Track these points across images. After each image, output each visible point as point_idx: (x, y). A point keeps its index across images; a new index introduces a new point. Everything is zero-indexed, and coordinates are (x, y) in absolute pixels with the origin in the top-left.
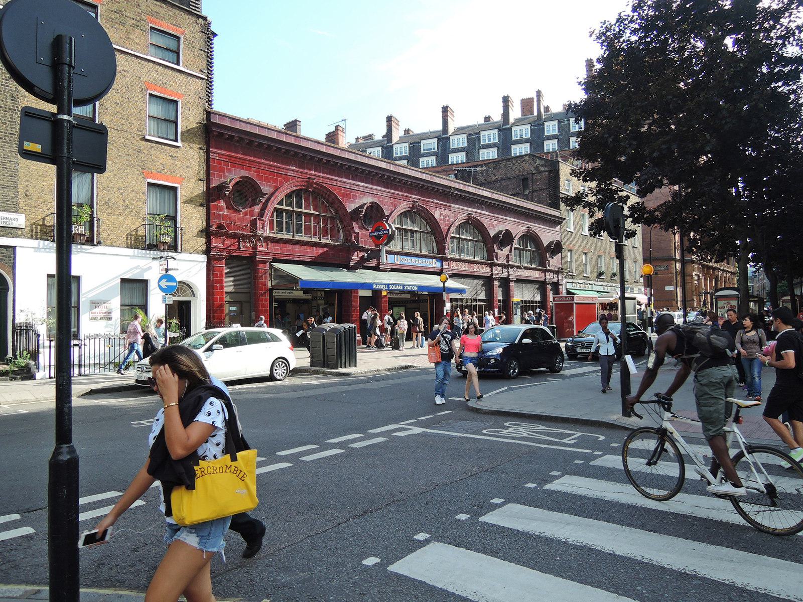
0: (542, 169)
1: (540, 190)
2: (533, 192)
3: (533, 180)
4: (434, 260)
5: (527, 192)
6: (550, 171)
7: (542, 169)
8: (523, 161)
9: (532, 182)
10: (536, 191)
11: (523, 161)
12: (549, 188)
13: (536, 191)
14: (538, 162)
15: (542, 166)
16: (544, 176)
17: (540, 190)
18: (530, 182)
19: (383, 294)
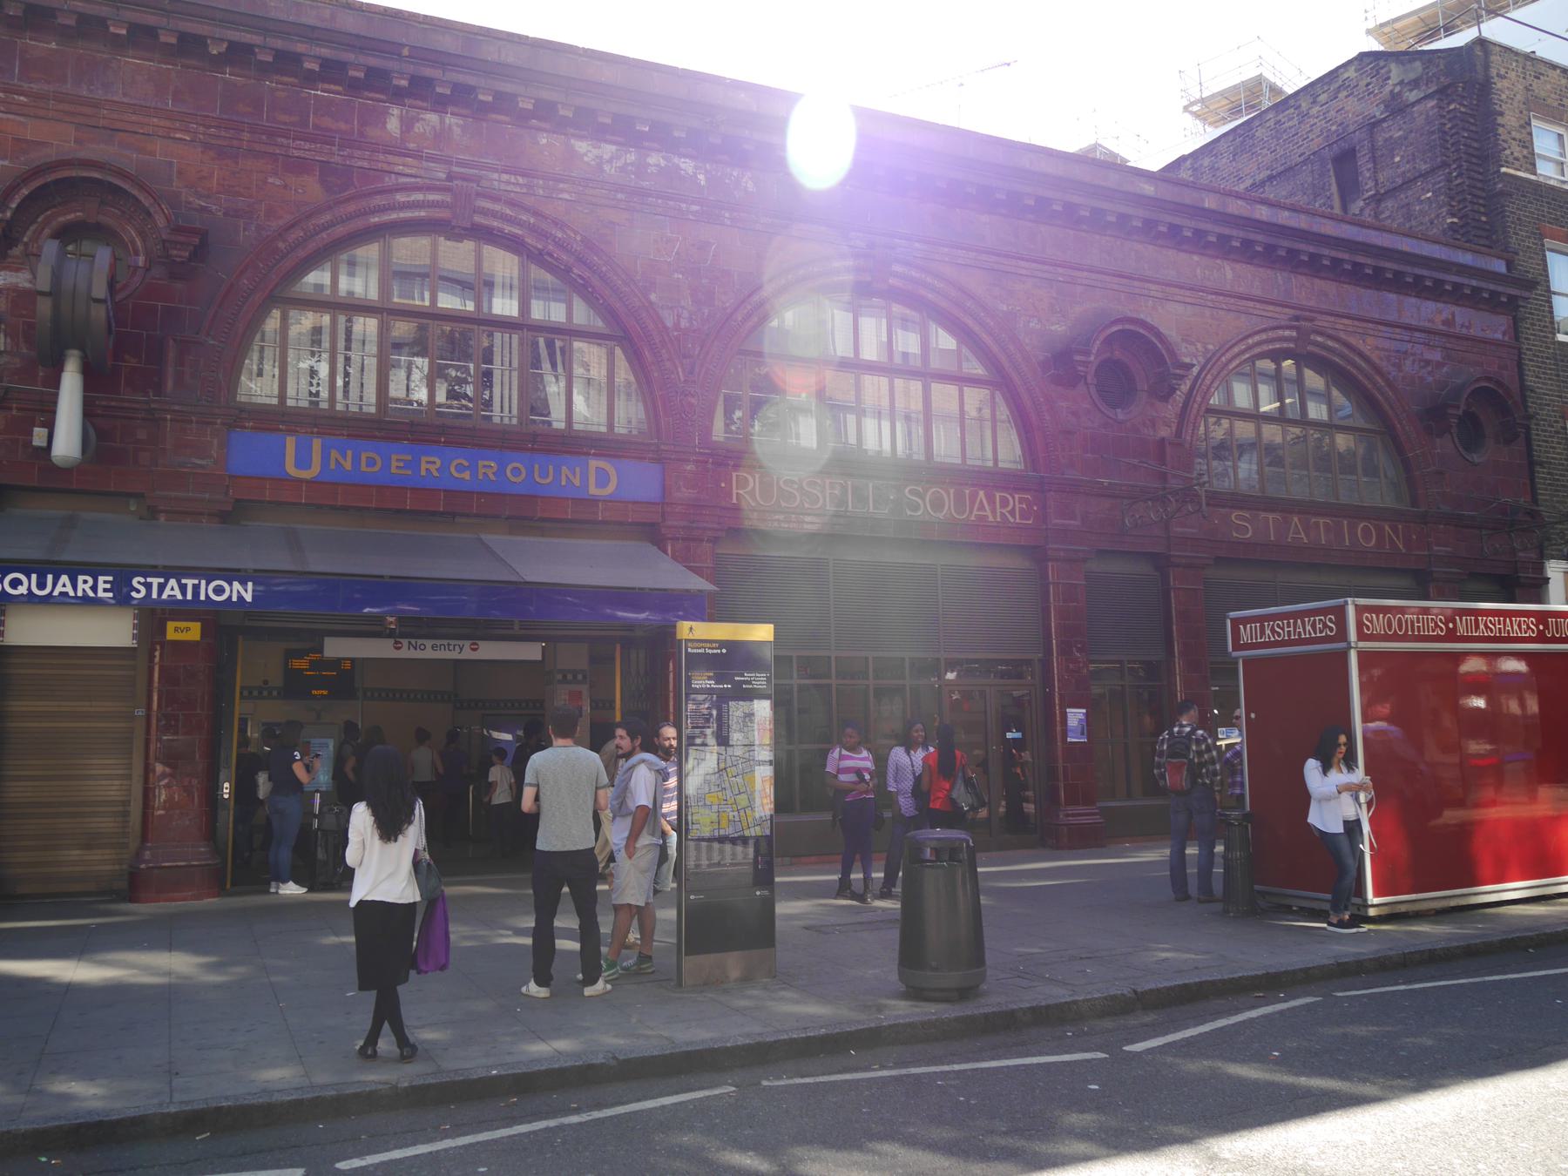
0: (1412, 96)
1: (1408, 183)
2: (1378, 199)
3: (1373, 149)
4: (594, 463)
5: (1356, 207)
6: (1442, 91)
7: (1412, 96)
8: (1339, 90)
9: (1374, 159)
10: (1392, 192)
11: (1339, 90)
12: (1445, 165)
13: (1392, 192)
14: (1396, 72)
15: (1415, 84)
16: (1420, 121)
17: (1408, 183)
18: (1363, 162)
19: (171, 635)
